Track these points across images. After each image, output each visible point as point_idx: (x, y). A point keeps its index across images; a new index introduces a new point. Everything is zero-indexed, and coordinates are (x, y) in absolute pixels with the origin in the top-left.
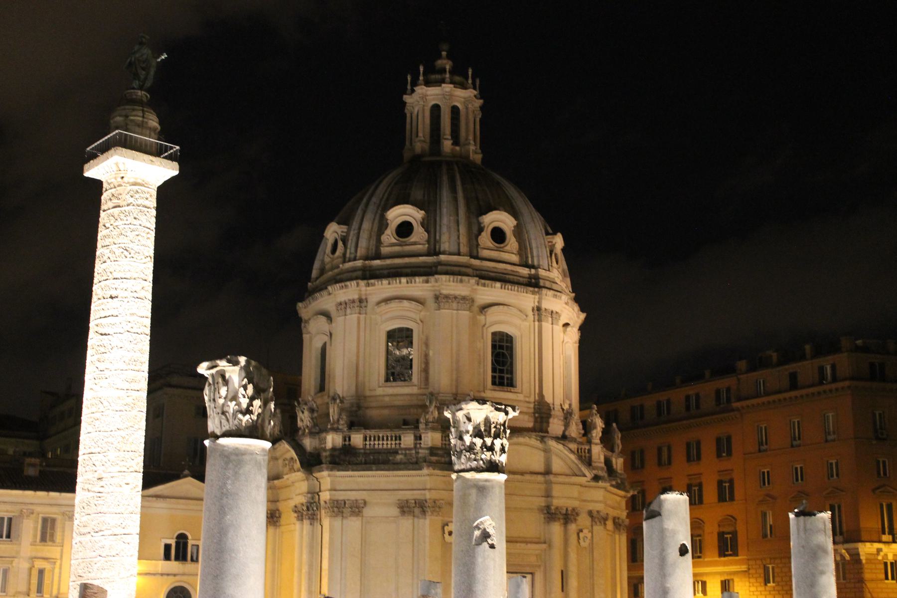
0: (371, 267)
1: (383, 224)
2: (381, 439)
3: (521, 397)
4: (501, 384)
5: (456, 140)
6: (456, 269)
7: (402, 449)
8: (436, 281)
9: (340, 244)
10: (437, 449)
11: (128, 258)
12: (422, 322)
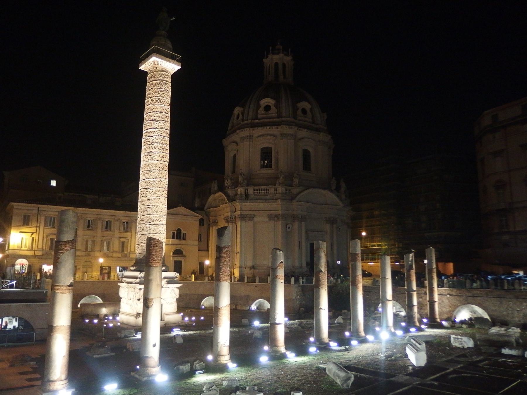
1: (259, 106)
2: (260, 190)
9: (241, 115)
11: (160, 103)
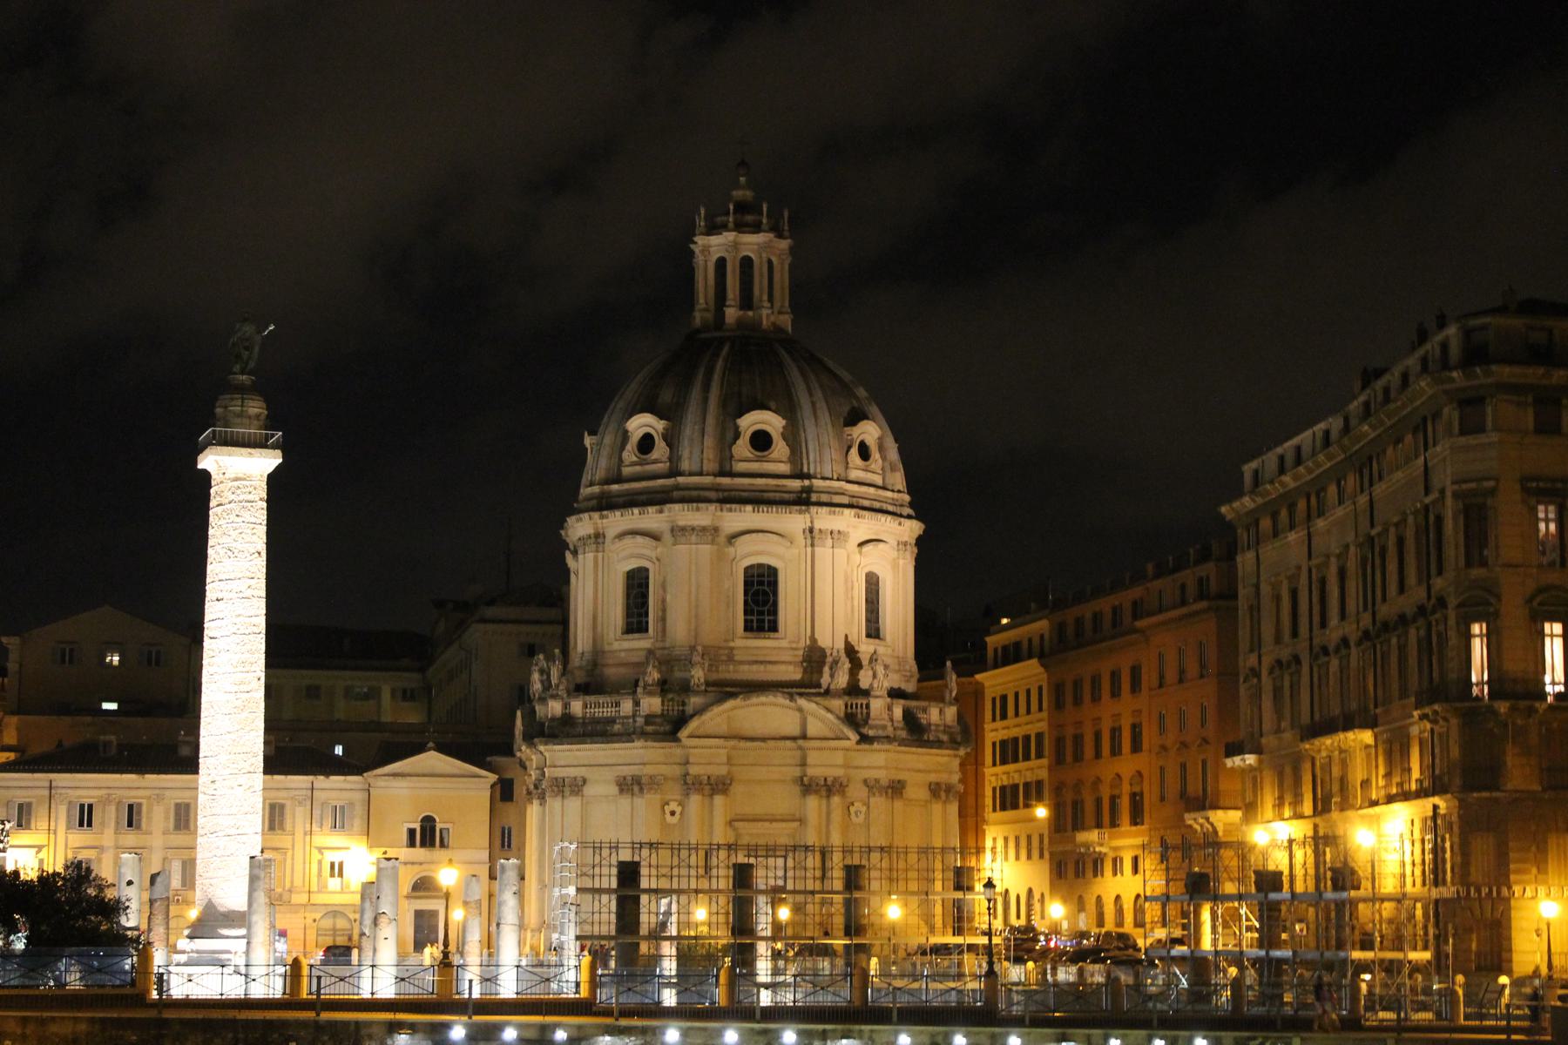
0: (610, 492)
1: (625, 436)
3: (784, 644)
4: (761, 629)
5: (747, 301)
6: (695, 493)
7: (620, 717)
8: (670, 511)
10: (655, 716)
12: (658, 560)
